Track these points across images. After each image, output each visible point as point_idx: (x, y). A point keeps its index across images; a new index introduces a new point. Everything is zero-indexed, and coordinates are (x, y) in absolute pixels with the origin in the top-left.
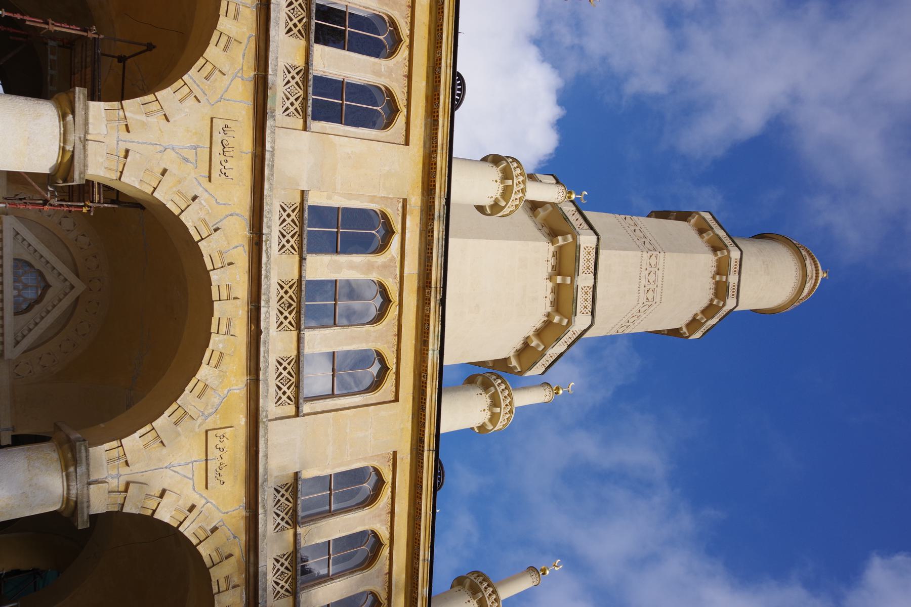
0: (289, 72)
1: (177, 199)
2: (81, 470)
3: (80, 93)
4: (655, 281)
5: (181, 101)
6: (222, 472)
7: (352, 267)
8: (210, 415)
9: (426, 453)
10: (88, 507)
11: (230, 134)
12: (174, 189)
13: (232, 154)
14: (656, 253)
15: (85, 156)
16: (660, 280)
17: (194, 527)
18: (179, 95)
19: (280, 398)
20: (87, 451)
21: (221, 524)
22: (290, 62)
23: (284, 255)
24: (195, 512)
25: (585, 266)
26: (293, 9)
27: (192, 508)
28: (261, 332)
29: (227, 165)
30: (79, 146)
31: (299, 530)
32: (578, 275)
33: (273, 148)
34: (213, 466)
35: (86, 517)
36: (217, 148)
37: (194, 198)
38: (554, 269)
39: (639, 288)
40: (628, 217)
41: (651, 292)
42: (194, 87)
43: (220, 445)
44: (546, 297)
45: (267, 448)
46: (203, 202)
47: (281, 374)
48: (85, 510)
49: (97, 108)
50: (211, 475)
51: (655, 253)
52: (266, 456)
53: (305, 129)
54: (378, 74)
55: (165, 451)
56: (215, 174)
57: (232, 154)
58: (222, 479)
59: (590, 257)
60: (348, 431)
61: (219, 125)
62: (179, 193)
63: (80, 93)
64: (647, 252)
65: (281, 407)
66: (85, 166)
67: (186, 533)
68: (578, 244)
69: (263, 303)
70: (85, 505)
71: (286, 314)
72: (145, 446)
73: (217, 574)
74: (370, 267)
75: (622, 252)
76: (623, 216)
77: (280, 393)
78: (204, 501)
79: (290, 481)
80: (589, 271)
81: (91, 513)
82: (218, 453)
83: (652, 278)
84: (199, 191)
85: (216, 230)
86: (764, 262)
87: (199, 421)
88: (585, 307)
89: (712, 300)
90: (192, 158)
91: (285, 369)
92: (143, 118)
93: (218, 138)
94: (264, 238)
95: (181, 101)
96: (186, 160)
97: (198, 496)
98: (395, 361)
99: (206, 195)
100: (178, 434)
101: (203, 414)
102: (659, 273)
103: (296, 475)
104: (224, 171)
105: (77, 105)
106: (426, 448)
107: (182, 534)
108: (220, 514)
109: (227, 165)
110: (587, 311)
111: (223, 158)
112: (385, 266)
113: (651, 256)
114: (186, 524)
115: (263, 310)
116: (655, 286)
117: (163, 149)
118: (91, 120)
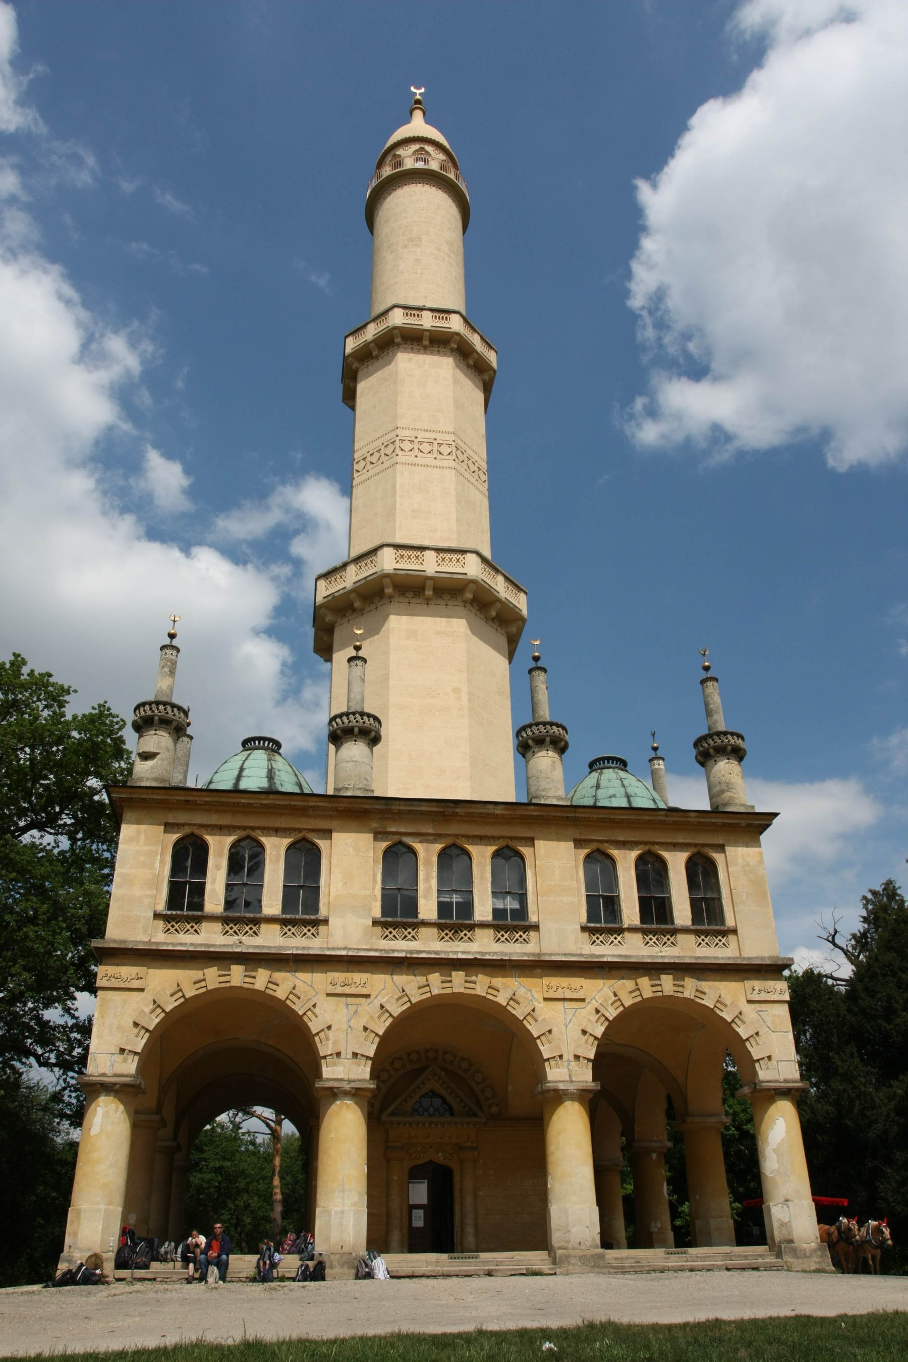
0: (286, 933)
1: (383, 1018)
2: (561, 1086)
3: (318, 1085)
4: (430, 443)
5: (317, 1017)
6: (574, 988)
7: (427, 879)
8: (532, 996)
9: (577, 815)
10: (586, 1082)
11: (336, 980)
12: (377, 1020)
13: (350, 979)
14: (398, 441)
15: (359, 1080)
16: (428, 435)
17: (611, 1009)
18: (313, 1017)
19: (524, 940)
20: (549, 1082)
21: (611, 988)
22: (279, 932)
23: (420, 936)
24: (600, 1009)
25: (415, 562)
26: (239, 930)
27: (597, 1011)
28: (476, 959)
29: (358, 982)
30: (353, 1085)
31: (626, 926)
32: (425, 571)
33: (345, 949)
34: (568, 995)
35: (593, 1084)
36: (347, 990)
37: (382, 1007)
38: (417, 594)
39: (437, 467)
40: (356, 467)
41: (442, 449)
42: (306, 1007)
43: (555, 989)
44: (447, 605)
45: (559, 954)
46: (384, 1000)
47: (506, 939)
48: (588, 1084)
49: (328, 1072)
50: (575, 996)
51: (398, 443)
52: (565, 955)
53: (326, 922)
54: (278, 856)
55: (555, 1030)
56: (364, 991)
57: (350, 979)
58: (578, 988)
59: (406, 555)
60: (553, 883)
61: (331, 989)
62: (379, 1017)
63: (318, 1085)
64: (397, 455)
65: (530, 939)
66: (364, 1080)
67: (615, 1015)
68: (392, 572)
69: (455, 957)
70: (585, 1084)
71: (462, 934)
72: (550, 1042)
73: (648, 993)
74: (428, 862)
75: (398, 494)
76: (356, 475)
77: (521, 940)
78: (594, 1001)
79: (586, 935)
80: (421, 555)
81: (591, 1080)
82: (560, 990)
83: (426, 447)
84: (377, 1003)
85: (403, 991)
86: (405, 246)
87: (536, 1004)
88: (458, 560)
89: (452, 350)
90: (355, 1007)
91: (503, 936)
92: (330, 1043)
93: (339, 990)
94: (409, 956)
95: (317, 1017)
96: (356, 1012)
97: (589, 1005)
98: (501, 840)
99: (379, 997)
100: (544, 1019)
101: (531, 1001)
102: (421, 435)
103: (584, 929)
104: (362, 985)
105: (327, 1086)
106: (573, 815)
107: (615, 1019)
108: (605, 989)
109: (358, 982)
110: (462, 558)
111: (353, 985)
112: (427, 850)
113: (402, 450)
114: (607, 1015)
115: (460, 956)
116: (435, 443)
117: (349, 1029)
118: (335, 1077)
